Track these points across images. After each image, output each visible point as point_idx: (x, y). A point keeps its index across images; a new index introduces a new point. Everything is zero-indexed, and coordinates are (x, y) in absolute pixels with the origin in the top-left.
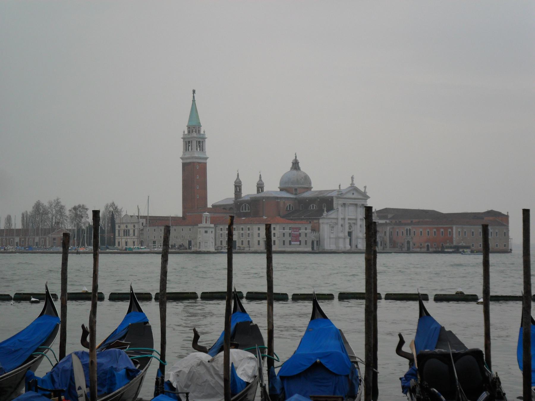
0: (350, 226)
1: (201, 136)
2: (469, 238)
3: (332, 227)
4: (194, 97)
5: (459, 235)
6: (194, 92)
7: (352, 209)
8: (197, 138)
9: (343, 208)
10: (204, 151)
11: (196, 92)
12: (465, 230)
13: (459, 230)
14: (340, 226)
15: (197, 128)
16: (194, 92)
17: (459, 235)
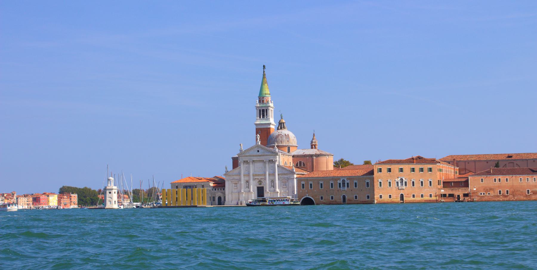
0: (258, 182)
1: (264, 105)
2: (315, 191)
3: (234, 183)
4: (264, 72)
5: (303, 187)
6: (264, 66)
7: (260, 165)
8: (258, 107)
9: (247, 165)
10: (268, 118)
11: (266, 67)
12: (310, 182)
13: (303, 183)
14: (243, 182)
15: (261, 98)
16: (264, 66)
17: (303, 187)
